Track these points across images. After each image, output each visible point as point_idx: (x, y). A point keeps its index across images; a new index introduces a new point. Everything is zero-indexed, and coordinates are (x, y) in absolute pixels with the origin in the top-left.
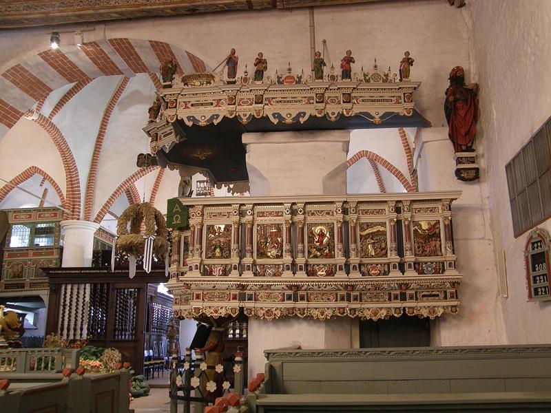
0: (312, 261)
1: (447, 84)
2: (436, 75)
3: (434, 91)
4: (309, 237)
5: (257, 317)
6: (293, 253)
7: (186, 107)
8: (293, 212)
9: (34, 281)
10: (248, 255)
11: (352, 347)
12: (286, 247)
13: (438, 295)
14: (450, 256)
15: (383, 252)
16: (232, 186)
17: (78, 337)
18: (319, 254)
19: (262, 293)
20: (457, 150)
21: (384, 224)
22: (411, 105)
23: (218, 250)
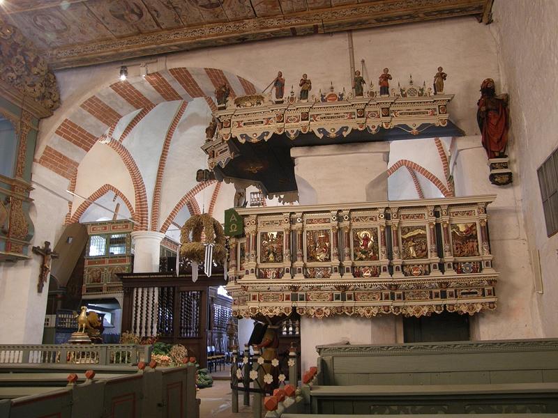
0: (358, 263)
1: (479, 95)
2: (468, 88)
3: (466, 103)
4: (354, 241)
5: (308, 316)
6: (340, 256)
7: (239, 126)
8: (340, 219)
9: (110, 286)
10: (299, 259)
11: (396, 342)
12: (333, 251)
13: (476, 293)
14: (486, 256)
15: (423, 253)
16: (282, 196)
17: (149, 335)
18: (364, 256)
19: (313, 293)
20: (490, 157)
21: (423, 228)
22: (445, 117)
23: (271, 255)
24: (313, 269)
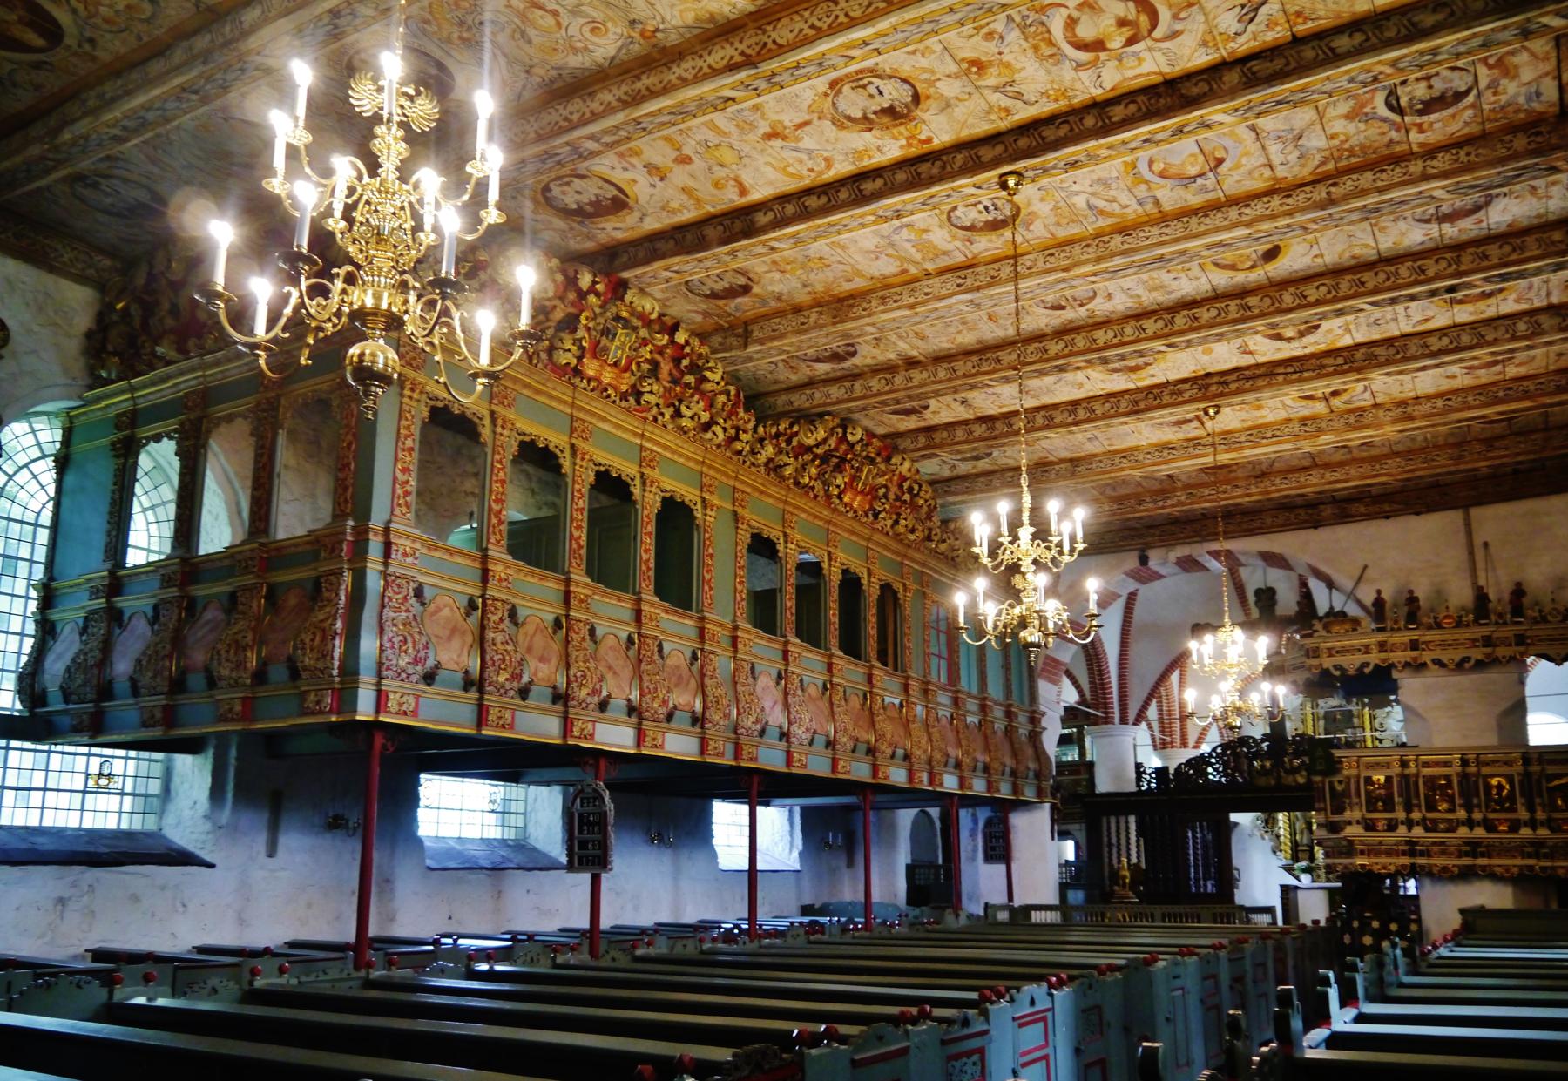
0: (1492, 816)
8: (1465, 762)
12: (1458, 801)
19: (1435, 848)
24: (1434, 821)
